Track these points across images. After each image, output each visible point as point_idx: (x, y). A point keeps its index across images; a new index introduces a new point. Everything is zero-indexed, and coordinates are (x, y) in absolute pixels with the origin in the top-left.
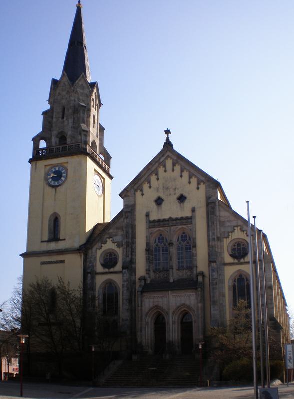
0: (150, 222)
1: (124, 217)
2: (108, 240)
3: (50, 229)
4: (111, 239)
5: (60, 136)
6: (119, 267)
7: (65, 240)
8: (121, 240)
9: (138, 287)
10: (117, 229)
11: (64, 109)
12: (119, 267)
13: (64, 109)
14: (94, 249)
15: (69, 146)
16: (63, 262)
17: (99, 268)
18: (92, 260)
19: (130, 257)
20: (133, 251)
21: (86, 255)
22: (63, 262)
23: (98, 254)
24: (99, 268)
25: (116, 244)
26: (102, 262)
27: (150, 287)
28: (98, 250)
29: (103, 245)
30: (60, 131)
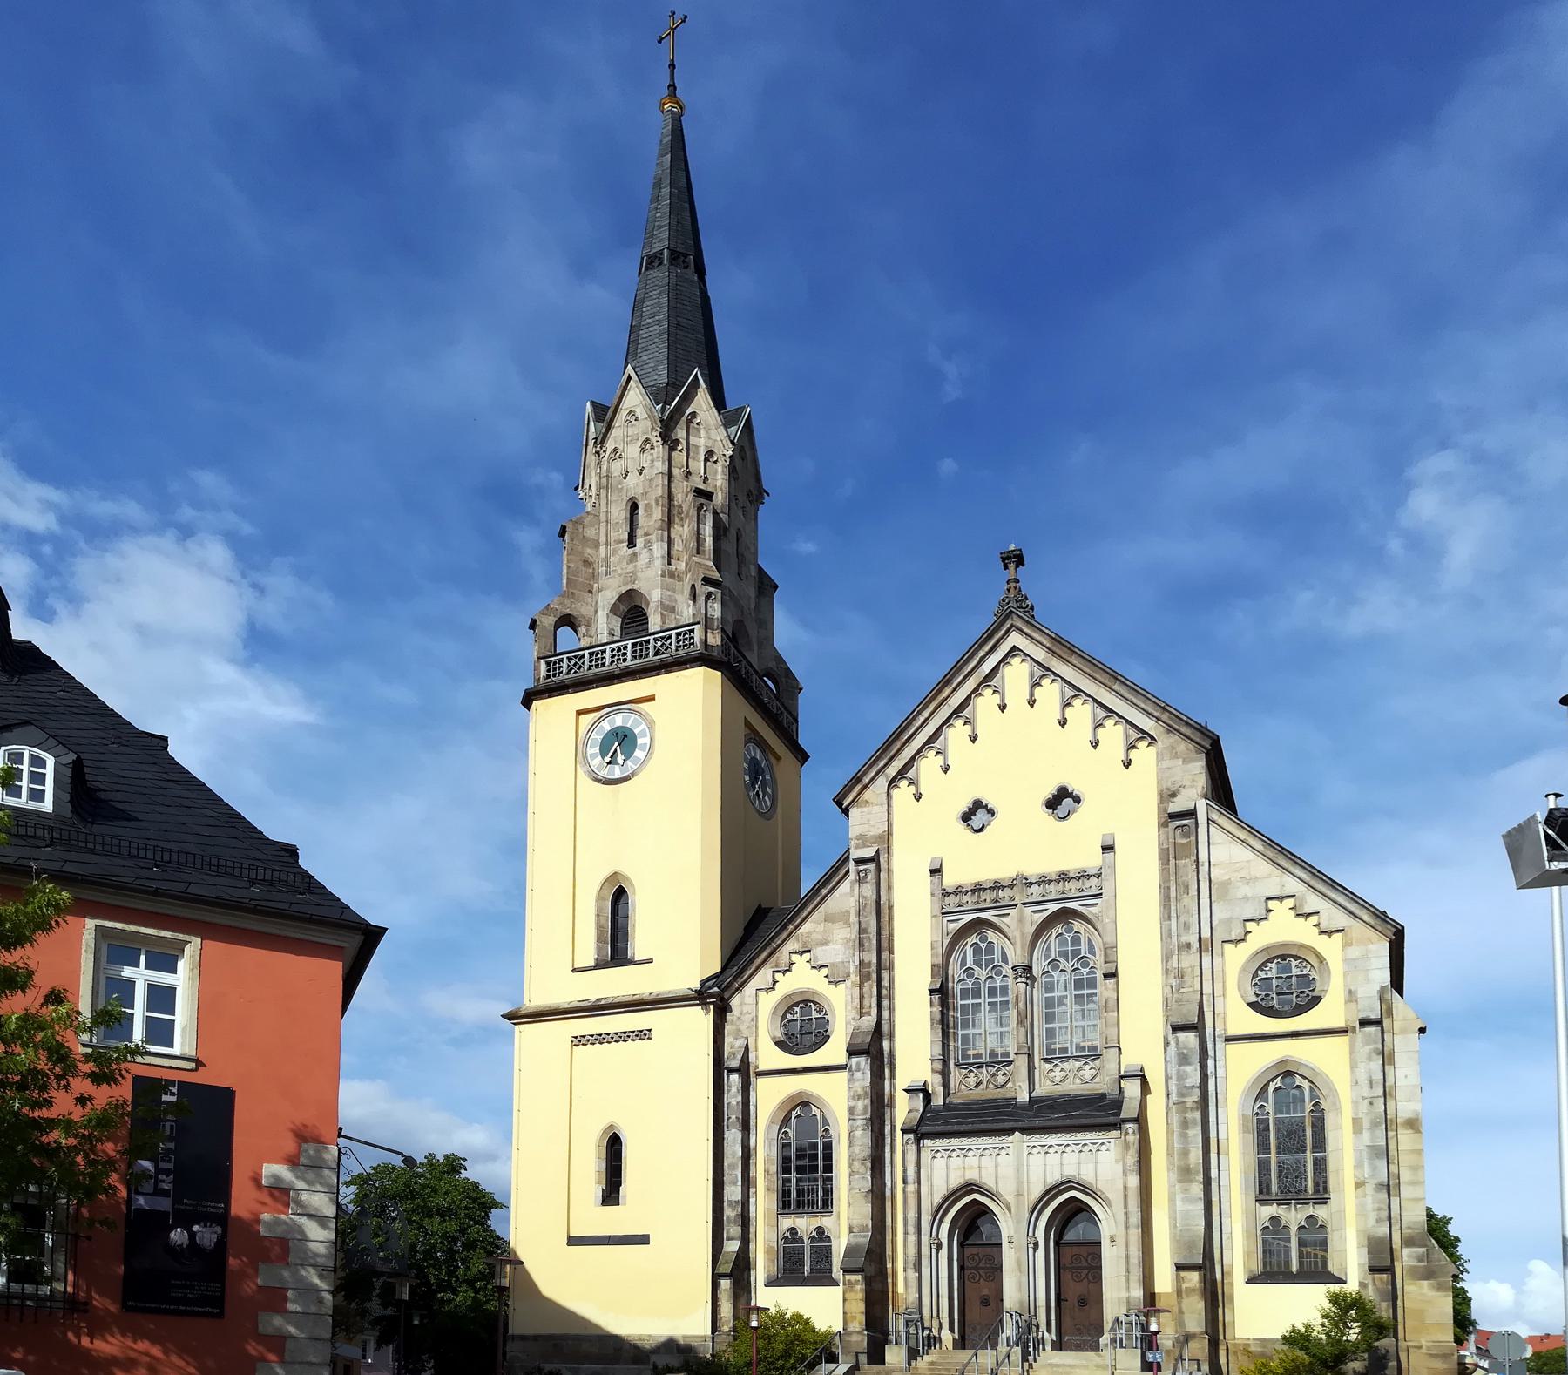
0: (946, 894)
1: (852, 876)
2: (795, 958)
3: (600, 928)
4: (806, 956)
5: (623, 608)
6: (834, 1051)
7: (651, 961)
8: (839, 959)
9: (904, 1109)
10: (828, 919)
11: (634, 507)
12: (834, 1051)
13: (634, 507)
14: (749, 989)
15: (656, 640)
16: (643, 1035)
17: (768, 1055)
18: (743, 1028)
19: (874, 1012)
20: (884, 996)
21: (722, 1011)
22: (643, 1035)
23: (759, 1006)
24: (768, 1055)
25: (824, 971)
26: (778, 1034)
27: (944, 1120)
28: (762, 994)
29: (778, 976)
30: (624, 589)
